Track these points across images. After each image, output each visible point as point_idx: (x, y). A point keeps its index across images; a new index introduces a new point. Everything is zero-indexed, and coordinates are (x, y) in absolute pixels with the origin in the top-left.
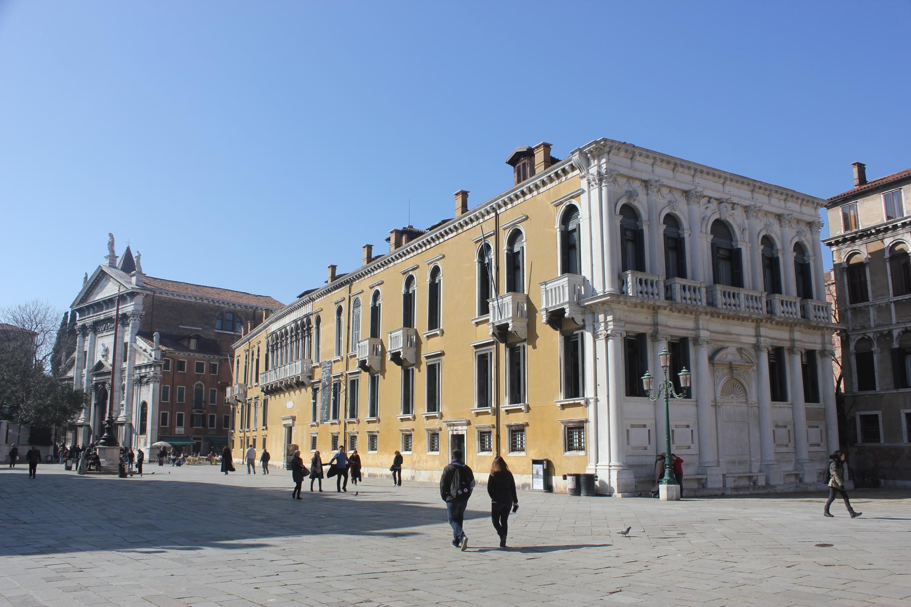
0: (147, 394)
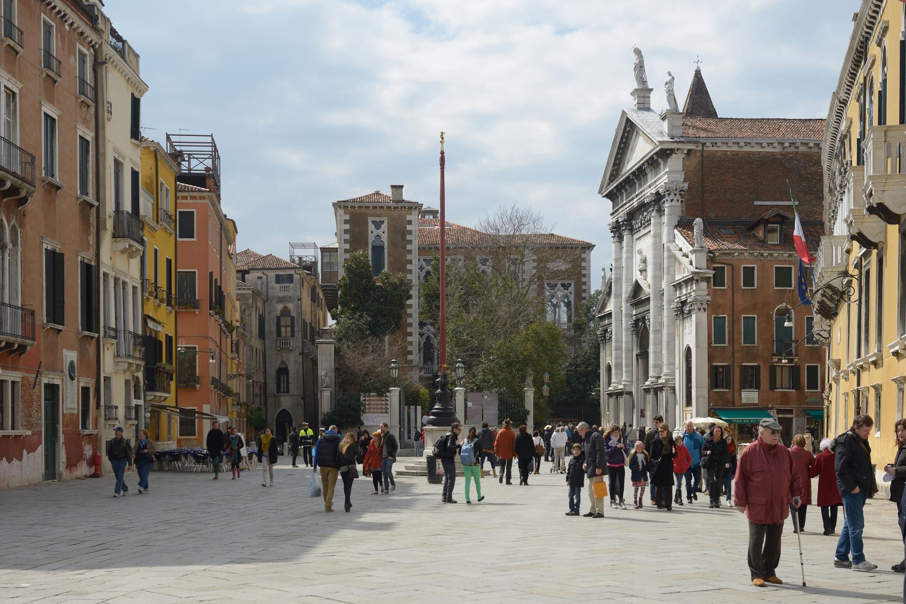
0: (690, 334)
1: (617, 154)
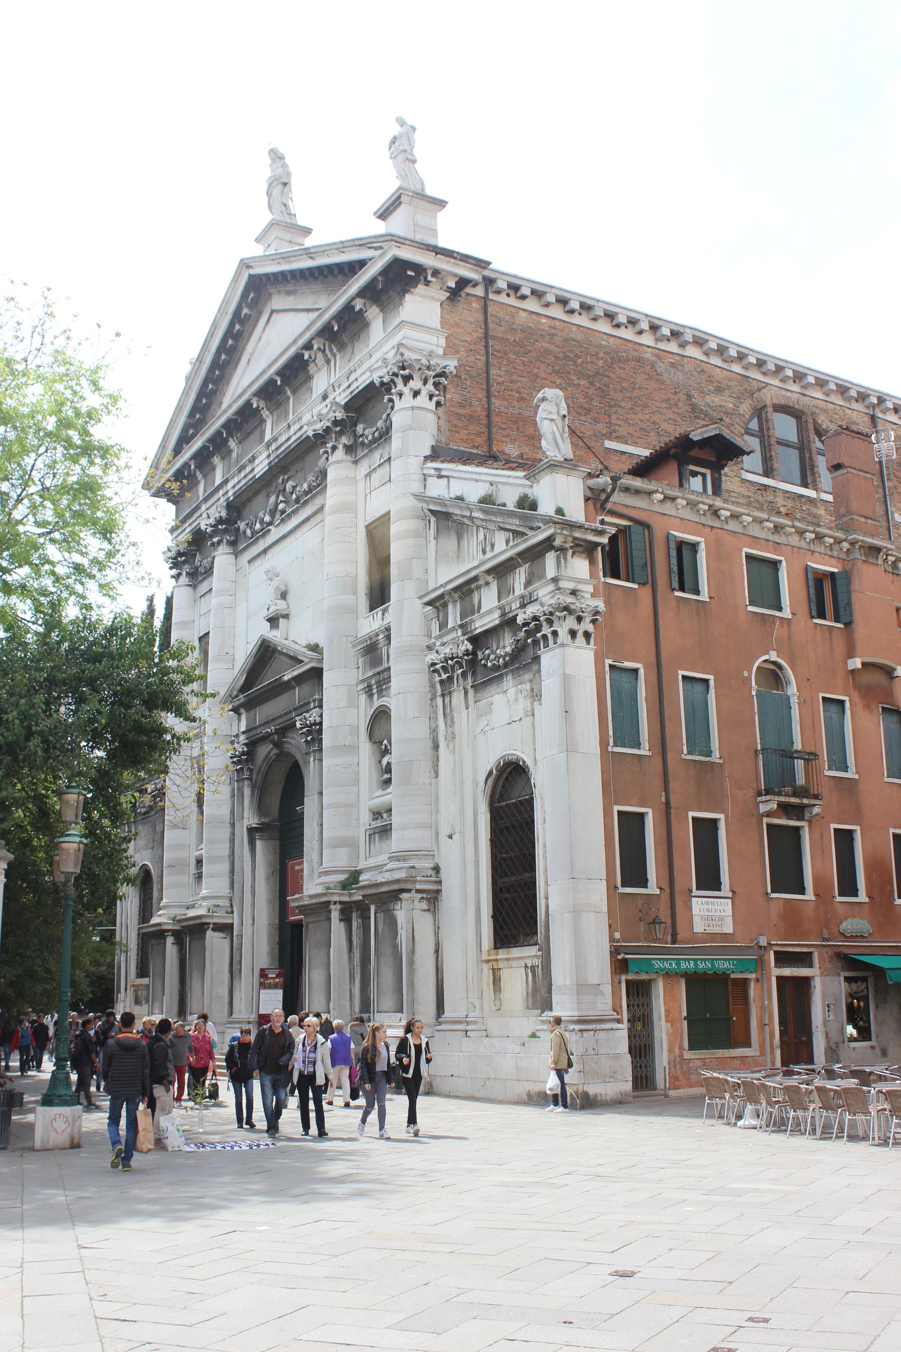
1: (205, 383)
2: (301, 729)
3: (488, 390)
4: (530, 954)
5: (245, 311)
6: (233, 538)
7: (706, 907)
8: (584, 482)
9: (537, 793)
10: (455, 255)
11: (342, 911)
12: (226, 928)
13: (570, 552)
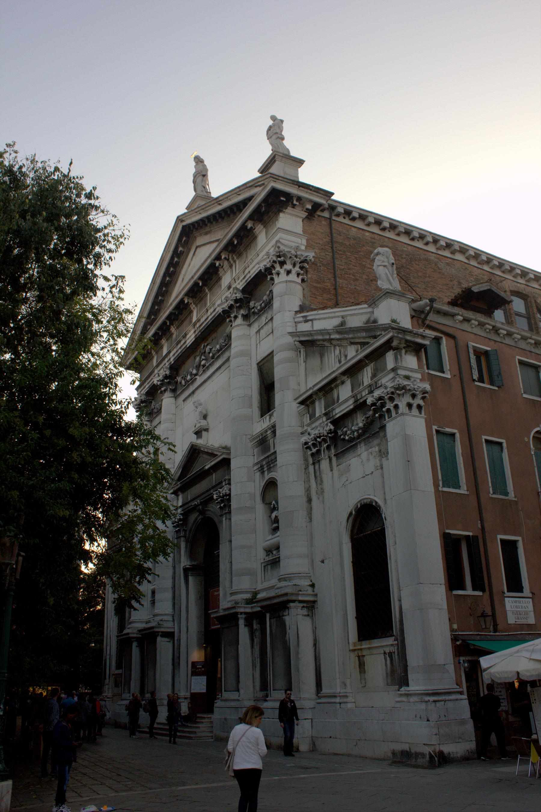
2: (217, 499)
3: (334, 274)
4: (388, 644)
5: (180, 249)
6: (174, 387)
7: (515, 604)
8: (409, 306)
9: (387, 524)
10: (311, 188)
11: (246, 619)
12: (170, 635)
13: (403, 351)
